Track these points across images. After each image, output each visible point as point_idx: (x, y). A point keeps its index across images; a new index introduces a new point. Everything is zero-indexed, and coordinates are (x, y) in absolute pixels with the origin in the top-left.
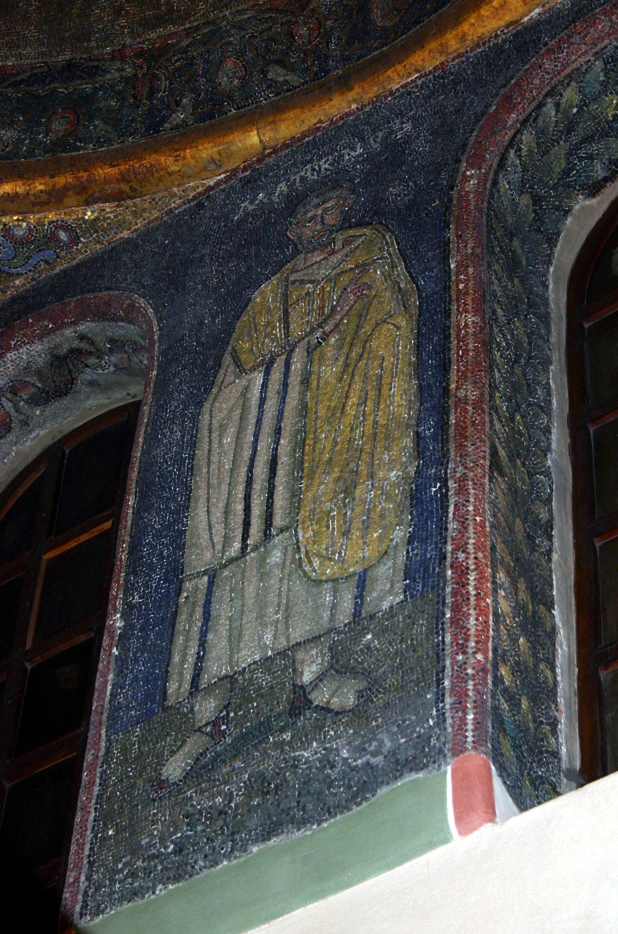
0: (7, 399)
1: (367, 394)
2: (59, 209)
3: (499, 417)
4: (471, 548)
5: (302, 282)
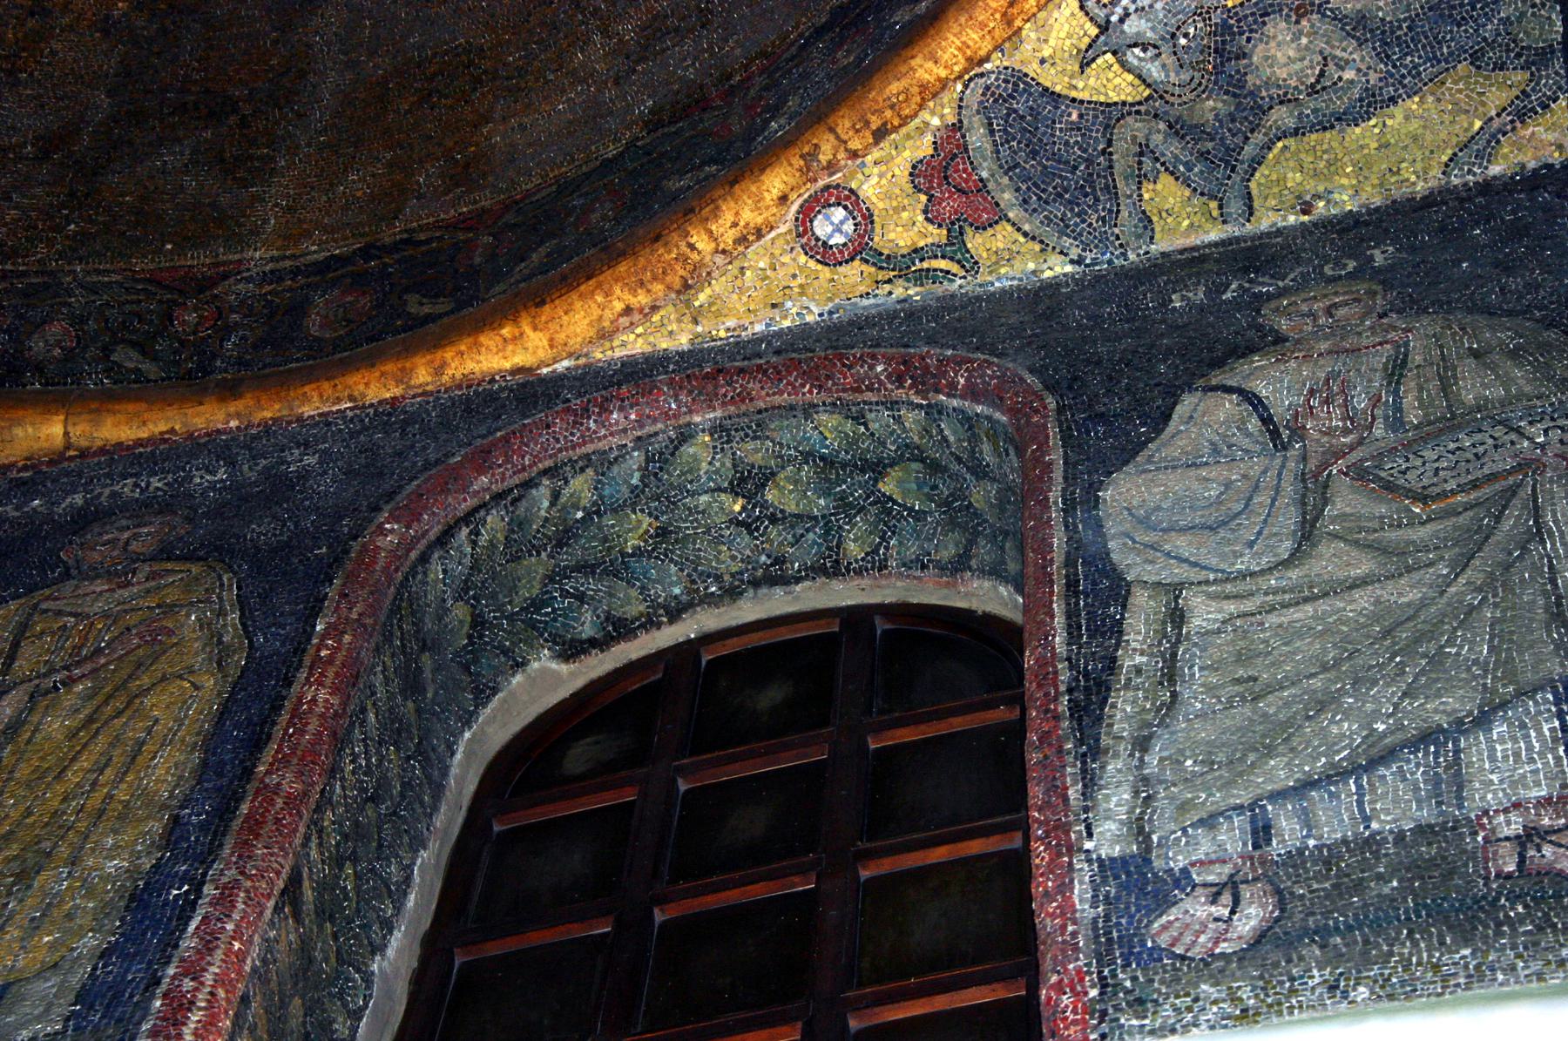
1: (110, 759)
3: (320, 845)
4: (208, 978)
5: (59, 613)
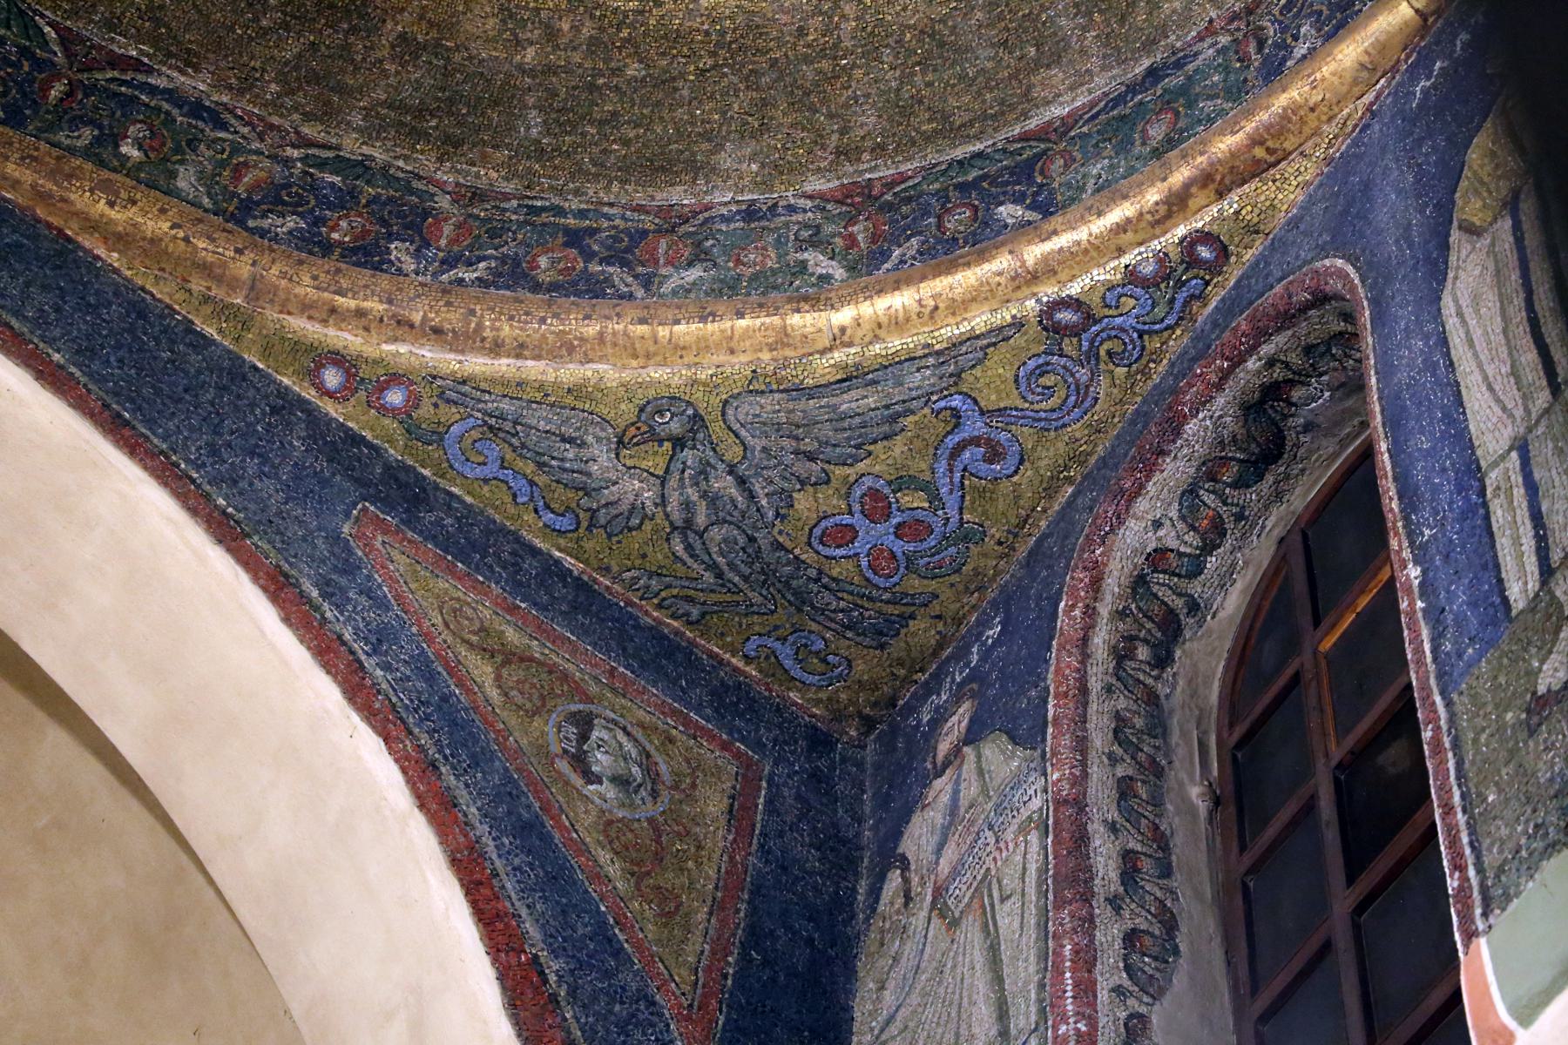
0: (1207, 490)
2: (1187, 219)
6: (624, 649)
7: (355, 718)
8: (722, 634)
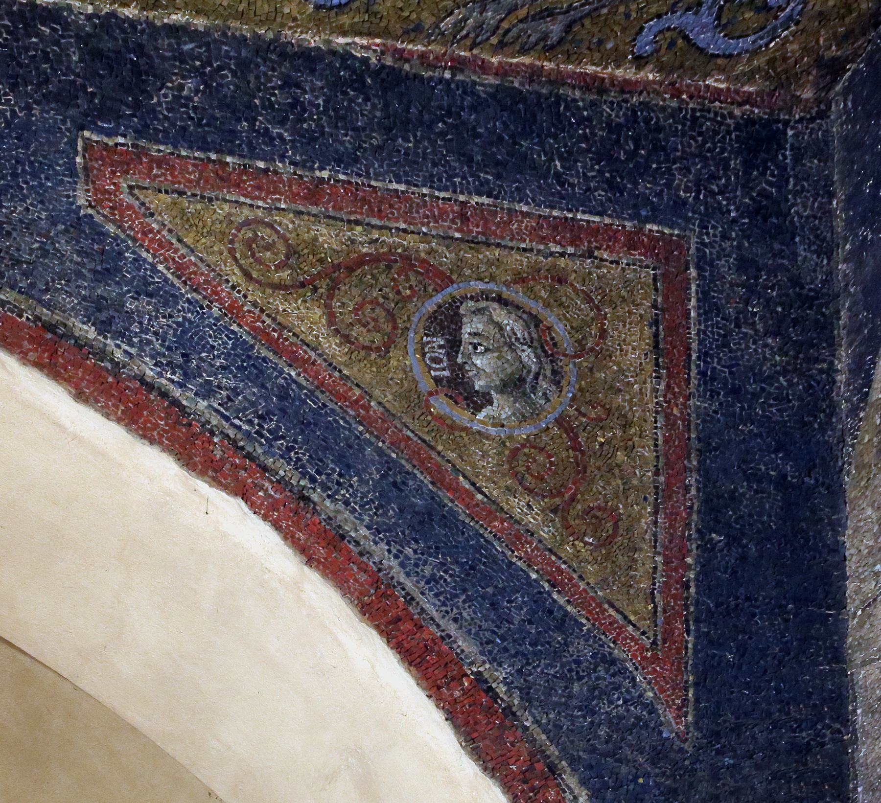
6: (470, 160)
7: (203, 486)
8: (601, 42)
